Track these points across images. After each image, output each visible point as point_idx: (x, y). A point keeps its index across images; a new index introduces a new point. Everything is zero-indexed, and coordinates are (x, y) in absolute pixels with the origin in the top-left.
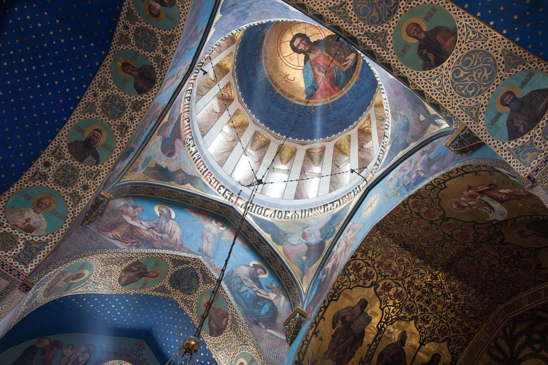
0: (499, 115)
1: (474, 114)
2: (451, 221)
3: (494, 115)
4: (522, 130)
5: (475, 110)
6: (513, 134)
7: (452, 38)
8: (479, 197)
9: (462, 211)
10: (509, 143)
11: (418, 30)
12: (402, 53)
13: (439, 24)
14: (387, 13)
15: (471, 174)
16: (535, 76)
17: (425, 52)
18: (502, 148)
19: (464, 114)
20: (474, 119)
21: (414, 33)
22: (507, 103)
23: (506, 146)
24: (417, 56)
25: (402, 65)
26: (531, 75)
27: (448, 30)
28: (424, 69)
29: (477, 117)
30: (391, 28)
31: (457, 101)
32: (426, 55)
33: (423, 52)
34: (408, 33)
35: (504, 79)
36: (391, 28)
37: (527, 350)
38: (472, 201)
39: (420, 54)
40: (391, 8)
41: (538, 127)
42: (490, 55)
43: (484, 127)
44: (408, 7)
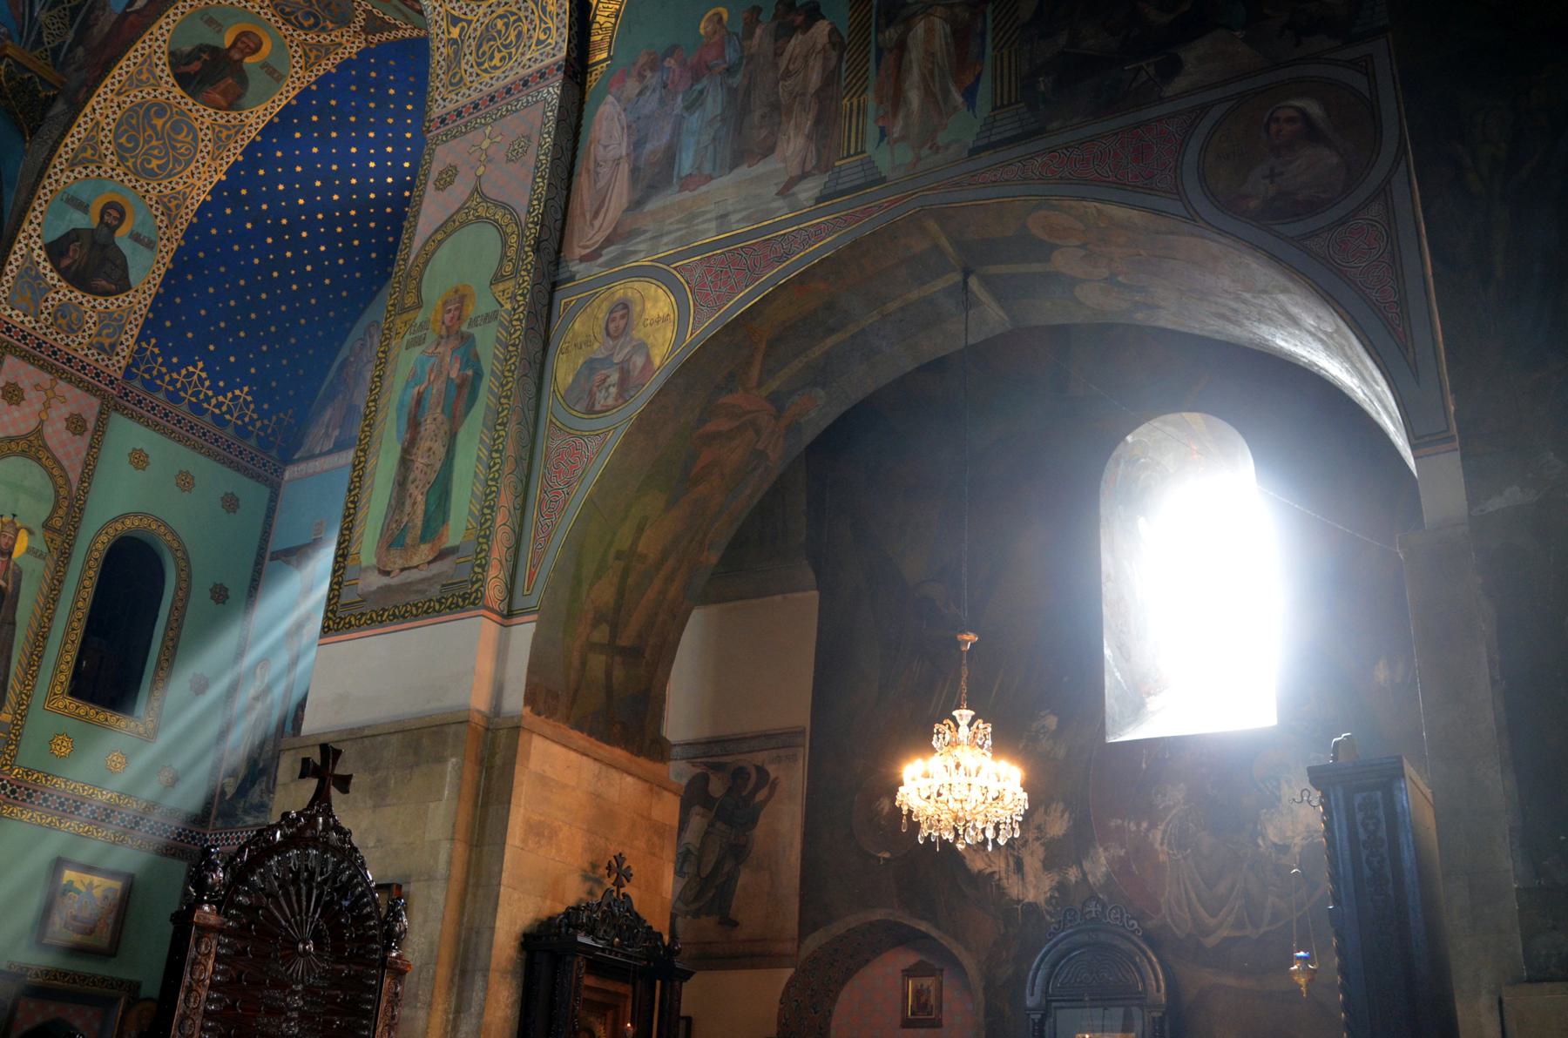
0: (84, 208)
1: (84, 155)
3: (84, 197)
4: (65, 262)
5: (93, 155)
6: (55, 251)
7: (224, 103)
10: (40, 248)
11: (248, 50)
12: (206, 17)
13: (252, 84)
14: (287, 10)
16: (147, 252)
17: (205, 56)
18: (31, 236)
19: (83, 135)
20: (75, 157)
21: (243, 42)
22: (106, 217)
23: (35, 243)
24: (197, 42)
25: (183, 13)
26: (150, 245)
27: (240, 96)
28: (172, 54)
29: (81, 163)
30: (258, 9)
31: (107, 117)
32: (199, 58)
33: (204, 53)
34: (244, 34)
35: (144, 197)
36: (258, 9)
39: (201, 49)
40: (296, 18)
41: (71, 292)
42: (187, 165)
43: (62, 184)
44: (292, 41)
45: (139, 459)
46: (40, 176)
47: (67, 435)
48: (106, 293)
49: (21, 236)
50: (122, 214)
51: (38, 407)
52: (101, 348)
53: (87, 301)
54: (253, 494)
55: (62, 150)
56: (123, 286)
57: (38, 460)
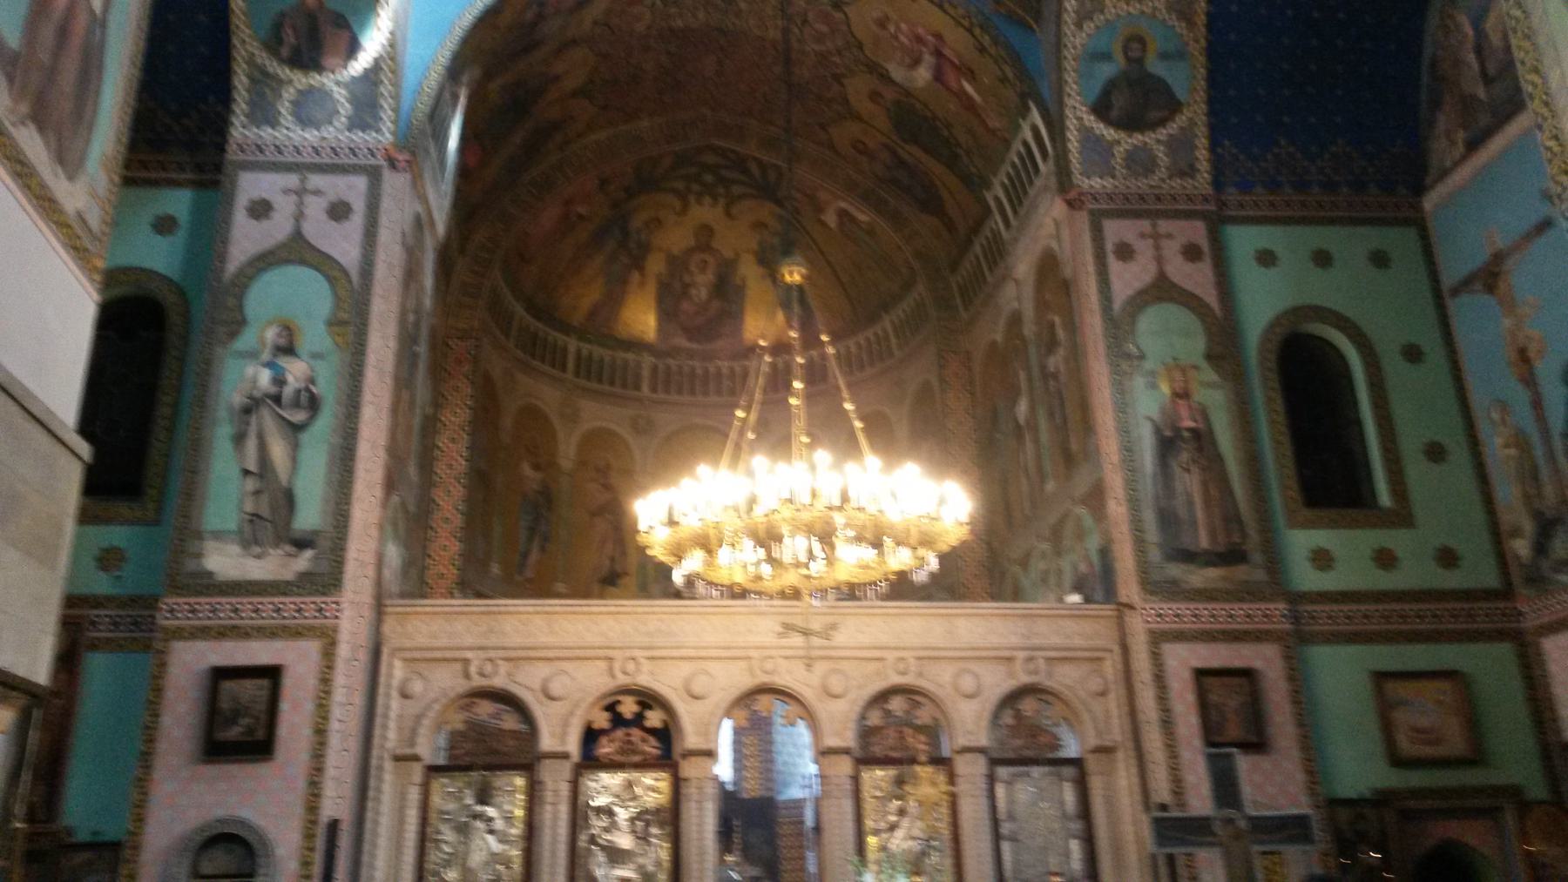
0: (1106, 57)
2: (839, 16)
4: (1115, 113)
8: (924, 49)
9: (874, 28)
15: (972, 40)
22: (1129, 54)
37: (680, 185)
38: (910, 40)
45: (1266, 258)
46: (1059, 51)
47: (1189, 267)
48: (1162, 122)
49: (1068, 112)
50: (1141, 41)
51: (1150, 253)
52: (1182, 174)
53: (1149, 138)
54: (1399, 241)
55: (1065, 17)
56: (1174, 106)
57: (1171, 300)
